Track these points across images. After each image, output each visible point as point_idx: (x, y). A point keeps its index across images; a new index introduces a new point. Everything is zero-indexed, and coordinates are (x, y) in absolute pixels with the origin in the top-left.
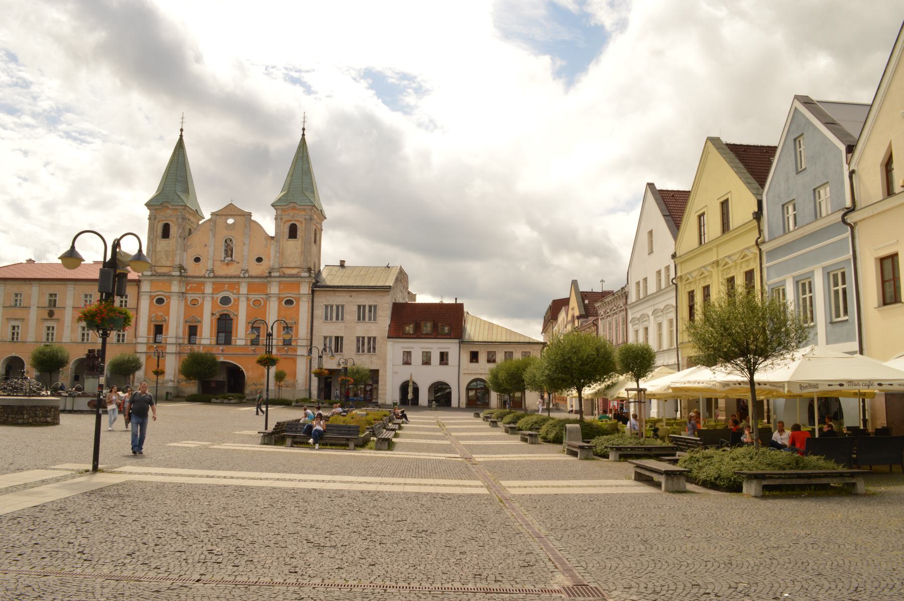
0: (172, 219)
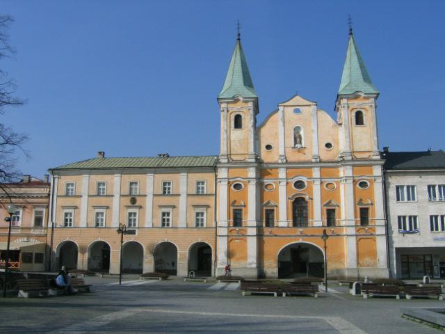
0: (245, 110)
